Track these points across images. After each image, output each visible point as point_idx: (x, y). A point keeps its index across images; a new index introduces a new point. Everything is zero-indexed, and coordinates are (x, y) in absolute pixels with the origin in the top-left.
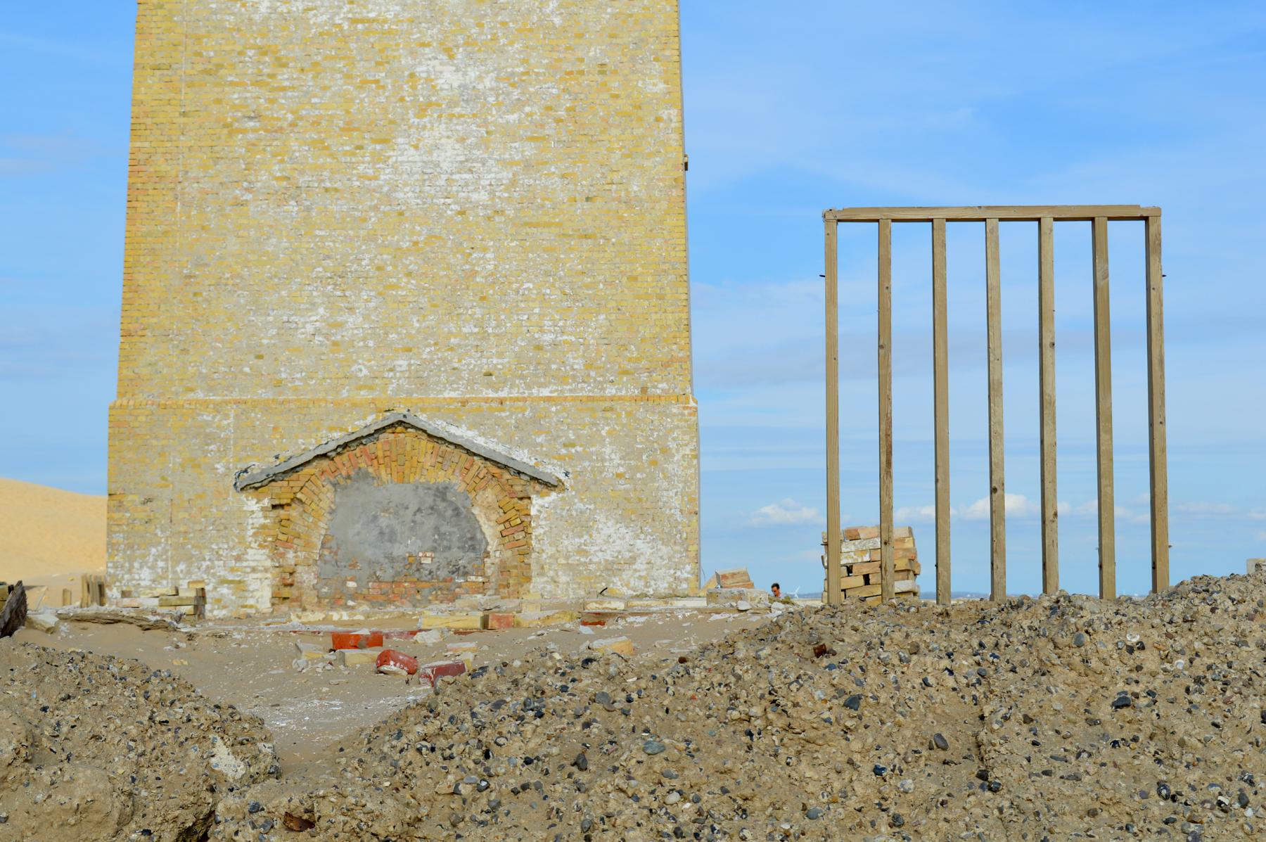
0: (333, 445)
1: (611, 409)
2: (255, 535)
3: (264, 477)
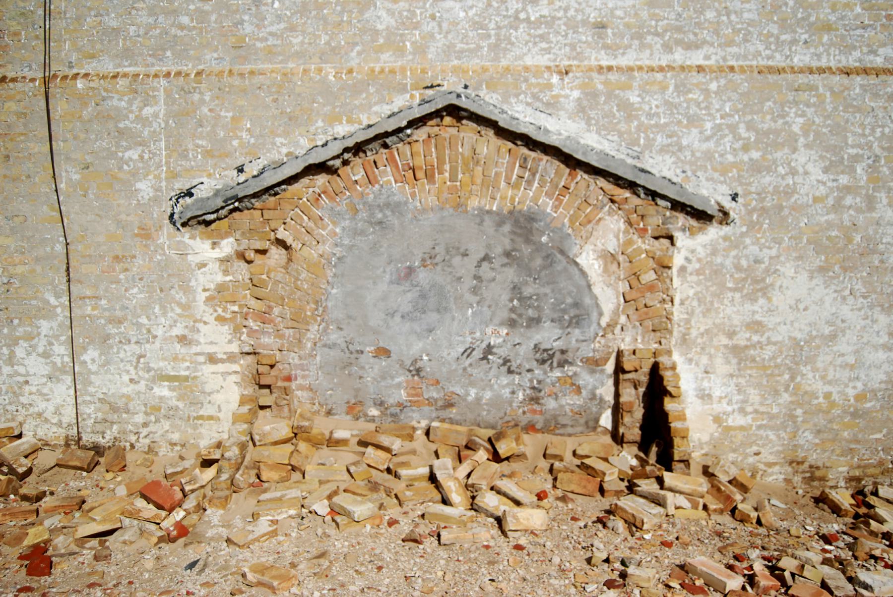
0: (335, 148)
1: (811, 88)
2: (209, 299)
3: (219, 203)
